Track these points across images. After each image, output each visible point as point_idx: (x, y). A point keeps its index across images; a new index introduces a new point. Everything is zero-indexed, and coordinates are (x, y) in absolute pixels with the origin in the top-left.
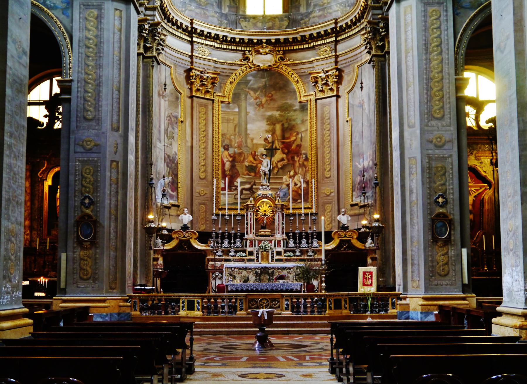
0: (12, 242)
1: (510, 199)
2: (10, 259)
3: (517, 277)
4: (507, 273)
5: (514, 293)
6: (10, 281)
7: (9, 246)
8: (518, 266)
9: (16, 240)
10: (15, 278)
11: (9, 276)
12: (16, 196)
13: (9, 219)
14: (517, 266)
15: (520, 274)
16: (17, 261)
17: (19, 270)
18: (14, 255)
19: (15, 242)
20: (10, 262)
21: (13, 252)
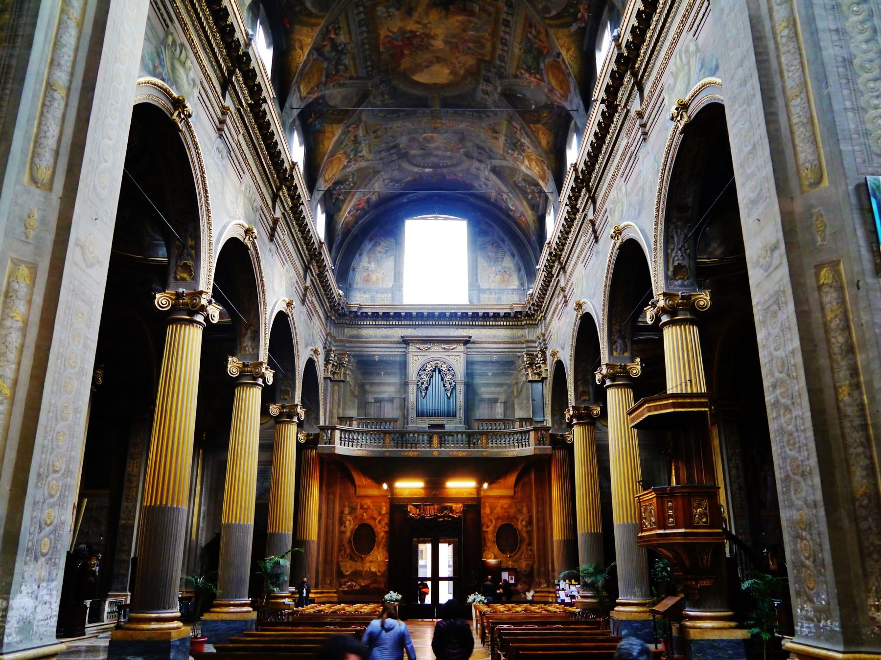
0: (802, 539)
1: (56, 476)
2: (803, 565)
3: (47, 598)
4: (24, 592)
5: (35, 623)
6: (810, 600)
7: (799, 546)
8: (53, 580)
9: (811, 535)
10: (818, 595)
11: (805, 592)
12: (798, 466)
13: (791, 506)
14: (50, 580)
15: (54, 592)
16: (818, 568)
17: (826, 582)
18: (811, 559)
19: (808, 537)
20: (804, 569)
21: (807, 555)
